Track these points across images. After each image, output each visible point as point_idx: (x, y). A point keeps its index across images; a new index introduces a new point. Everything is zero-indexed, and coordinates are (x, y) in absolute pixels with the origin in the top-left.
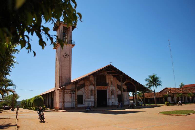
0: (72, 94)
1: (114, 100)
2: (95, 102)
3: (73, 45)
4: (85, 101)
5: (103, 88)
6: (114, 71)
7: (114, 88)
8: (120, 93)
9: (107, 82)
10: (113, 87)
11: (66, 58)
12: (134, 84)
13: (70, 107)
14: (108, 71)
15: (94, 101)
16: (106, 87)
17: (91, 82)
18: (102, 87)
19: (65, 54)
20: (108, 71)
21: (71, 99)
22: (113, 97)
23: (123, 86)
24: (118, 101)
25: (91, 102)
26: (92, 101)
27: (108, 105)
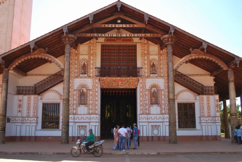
1: (162, 121)
2: (169, 122)
5: (121, 83)
6: (138, 25)
7: (161, 83)
8: (185, 96)
9: (139, 65)
10: (156, 79)
12: (224, 67)
14: (117, 26)
15: (168, 120)
16: (132, 79)
18: (119, 78)
20: (117, 26)
22: (155, 109)
24: (168, 124)
25: (77, 124)
26: (82, 120)
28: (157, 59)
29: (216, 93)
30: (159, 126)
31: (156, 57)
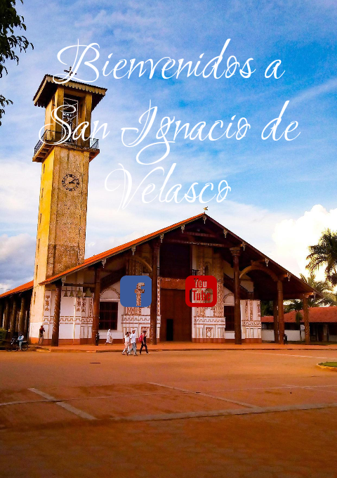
0: (84, 300)
3: (94, 153)
4: (123, 320)
8: (230, 301)
9: (194, 267)
11: (71, 190)
13: (78, 337)
17: (144, 268)
19: (70, 179)
20: (197, 234)
21: (80, 314)
23: (240, 280)
24: (225, 327)
25: (141, 326)
27: (193, 336)
28: (211, 262)
29: (255, 298)
30: (211, 328)
31: (210, 261)
